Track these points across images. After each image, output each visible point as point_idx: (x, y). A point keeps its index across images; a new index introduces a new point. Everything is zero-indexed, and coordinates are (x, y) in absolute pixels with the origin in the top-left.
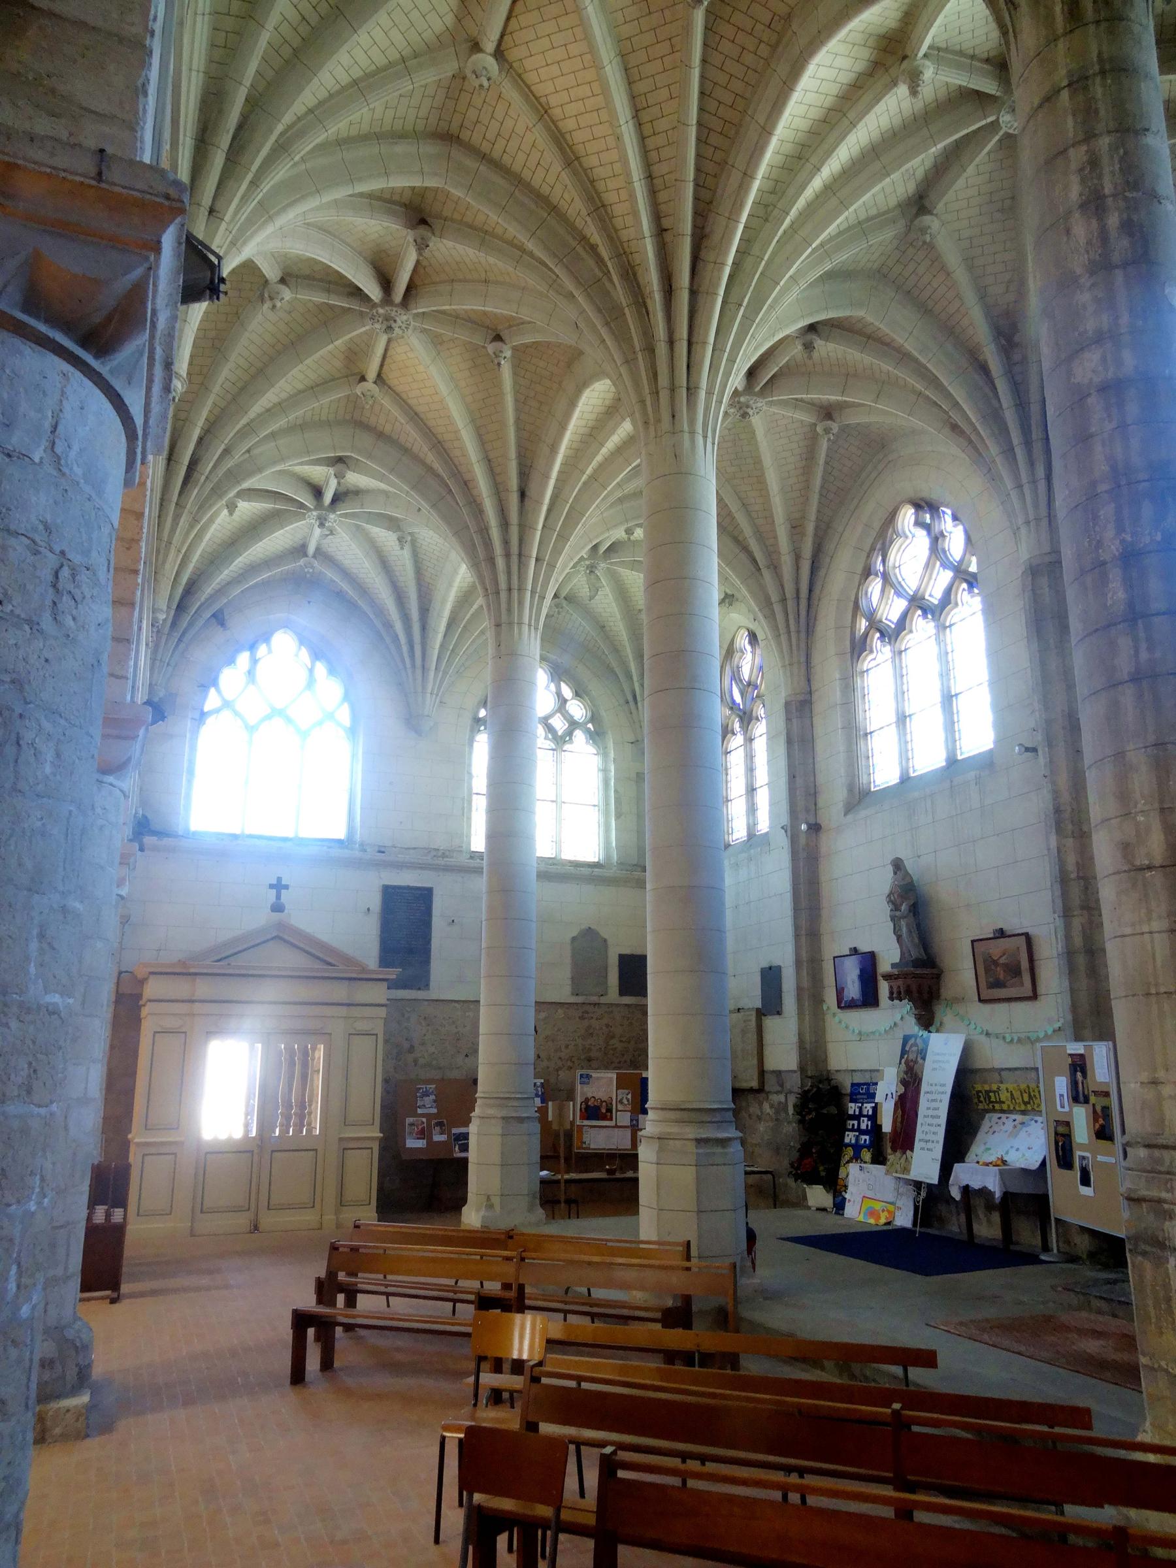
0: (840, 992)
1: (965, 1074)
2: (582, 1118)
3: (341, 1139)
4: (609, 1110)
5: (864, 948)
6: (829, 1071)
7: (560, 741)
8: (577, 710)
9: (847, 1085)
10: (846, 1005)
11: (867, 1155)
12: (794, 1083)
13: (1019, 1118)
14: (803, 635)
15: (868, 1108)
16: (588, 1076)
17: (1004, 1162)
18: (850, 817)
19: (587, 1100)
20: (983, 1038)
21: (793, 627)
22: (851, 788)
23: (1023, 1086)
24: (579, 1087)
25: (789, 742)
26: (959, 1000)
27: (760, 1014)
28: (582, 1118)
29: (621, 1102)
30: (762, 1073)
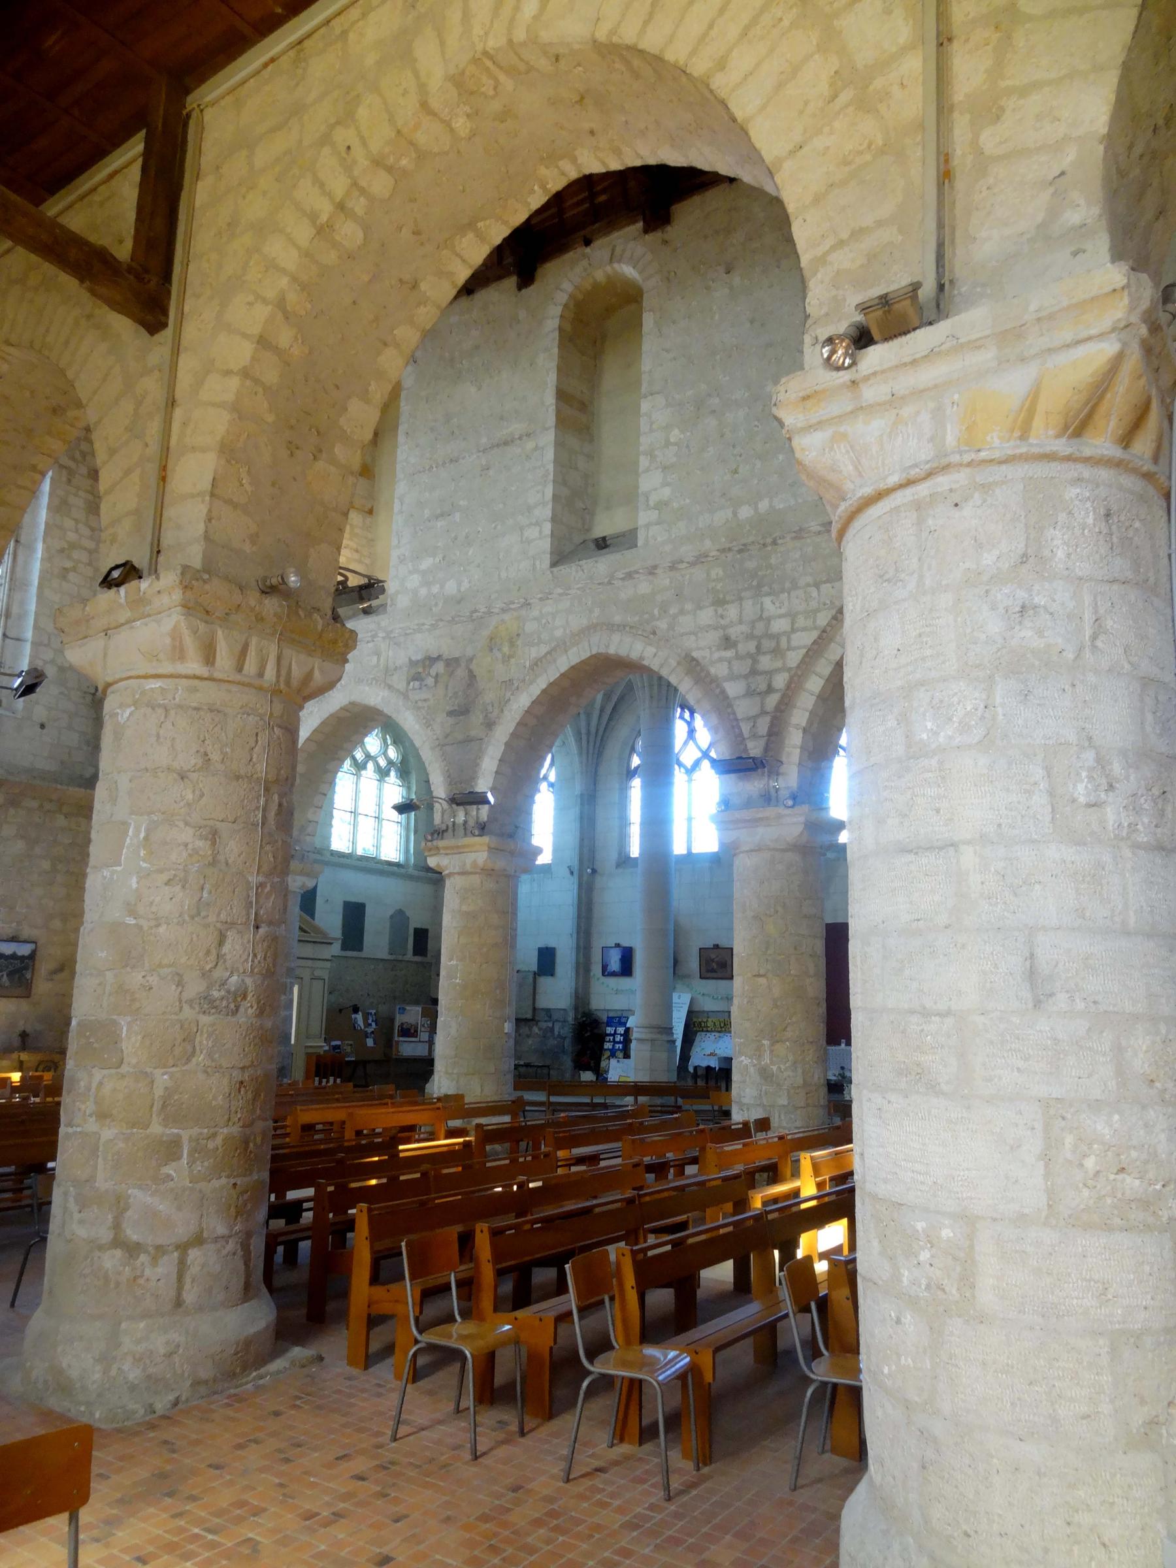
0: (604, 968)
1: (690, 1013)
2: (399, 1036)
3: (306, 1047)
4: (416, 1031)
5: (625, 944)
6: (590, 1010)
7: (383, 773)
8: (392, 753)
9: (605, 1019)
10: (606, 972)
11: (620, 1055)
12: (570, 1018)
13: (717, 1034)
14: (596, 756)
15: (621, 1030)
16: (404, 1009)
17: (716, 1055)
18: (620, 870)
19: (402, 1024)
20: (699, 997)
21: (591, 751)
22: (620, 854)
23: (722, 1020)
24: (398, 1016)
25: (581, 818)
26: (687, 976)
27: (536, 975)
28: (399, 1036)
29: (423, 1026)
30: (534, 1009)
